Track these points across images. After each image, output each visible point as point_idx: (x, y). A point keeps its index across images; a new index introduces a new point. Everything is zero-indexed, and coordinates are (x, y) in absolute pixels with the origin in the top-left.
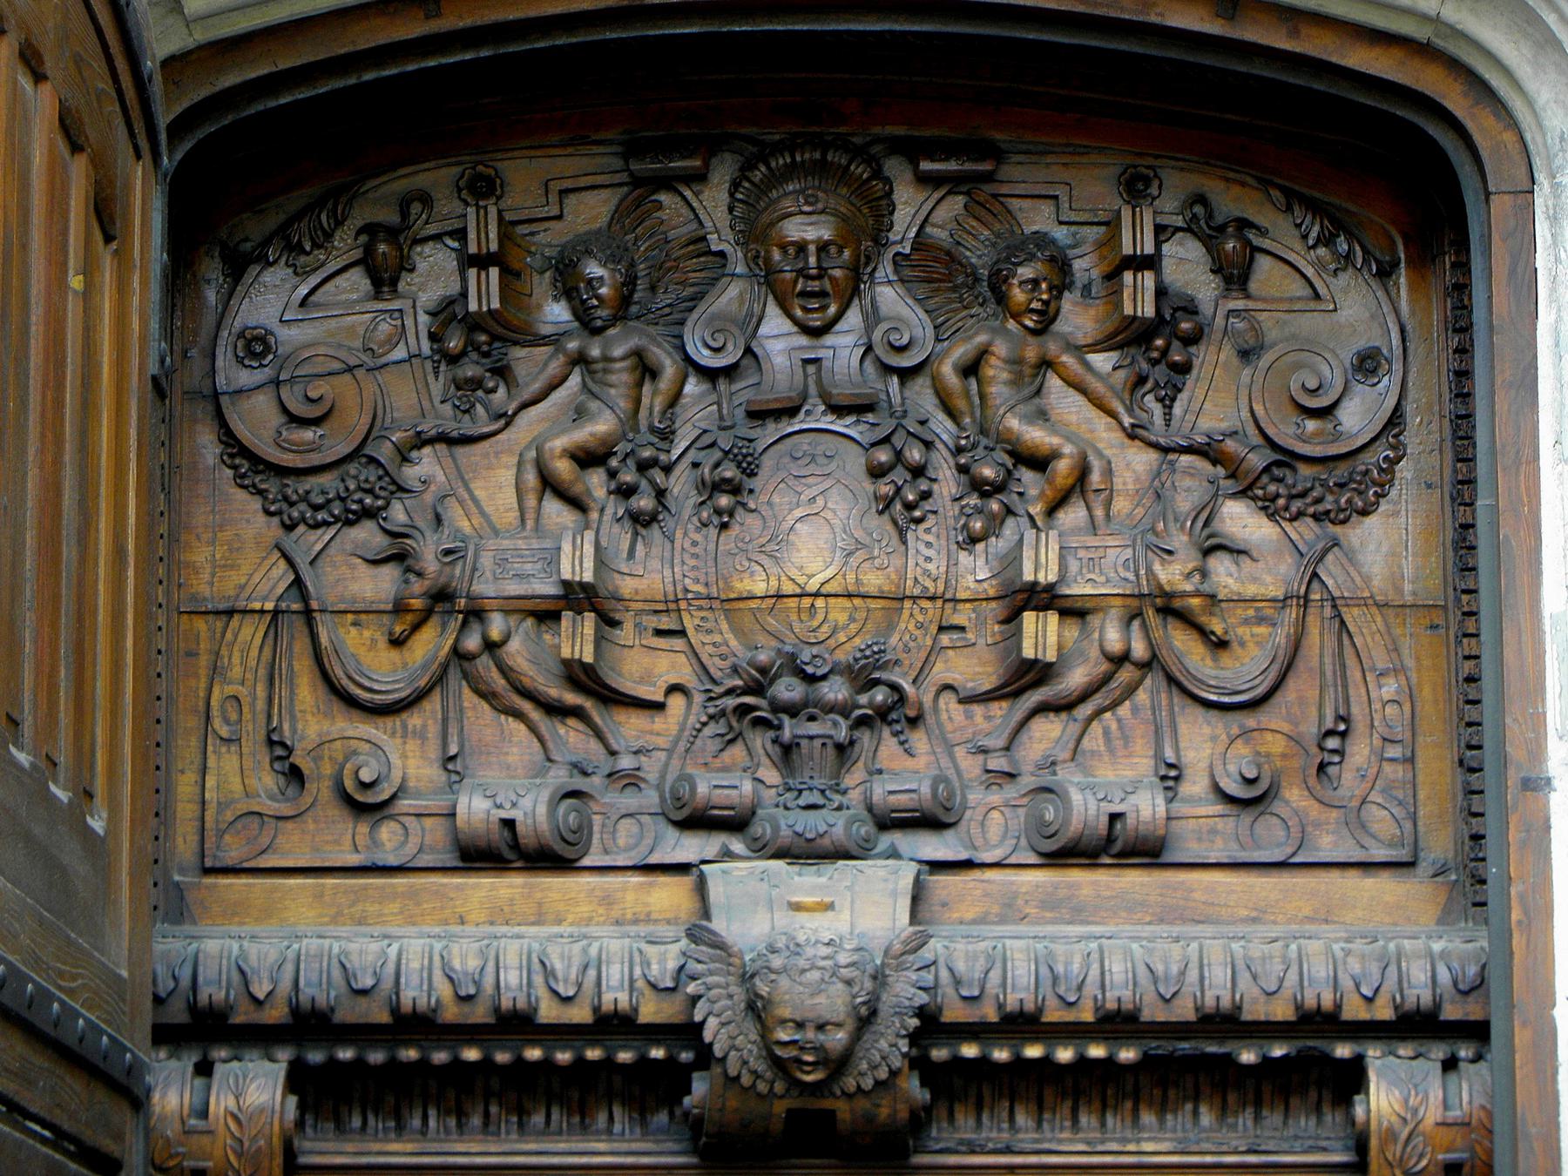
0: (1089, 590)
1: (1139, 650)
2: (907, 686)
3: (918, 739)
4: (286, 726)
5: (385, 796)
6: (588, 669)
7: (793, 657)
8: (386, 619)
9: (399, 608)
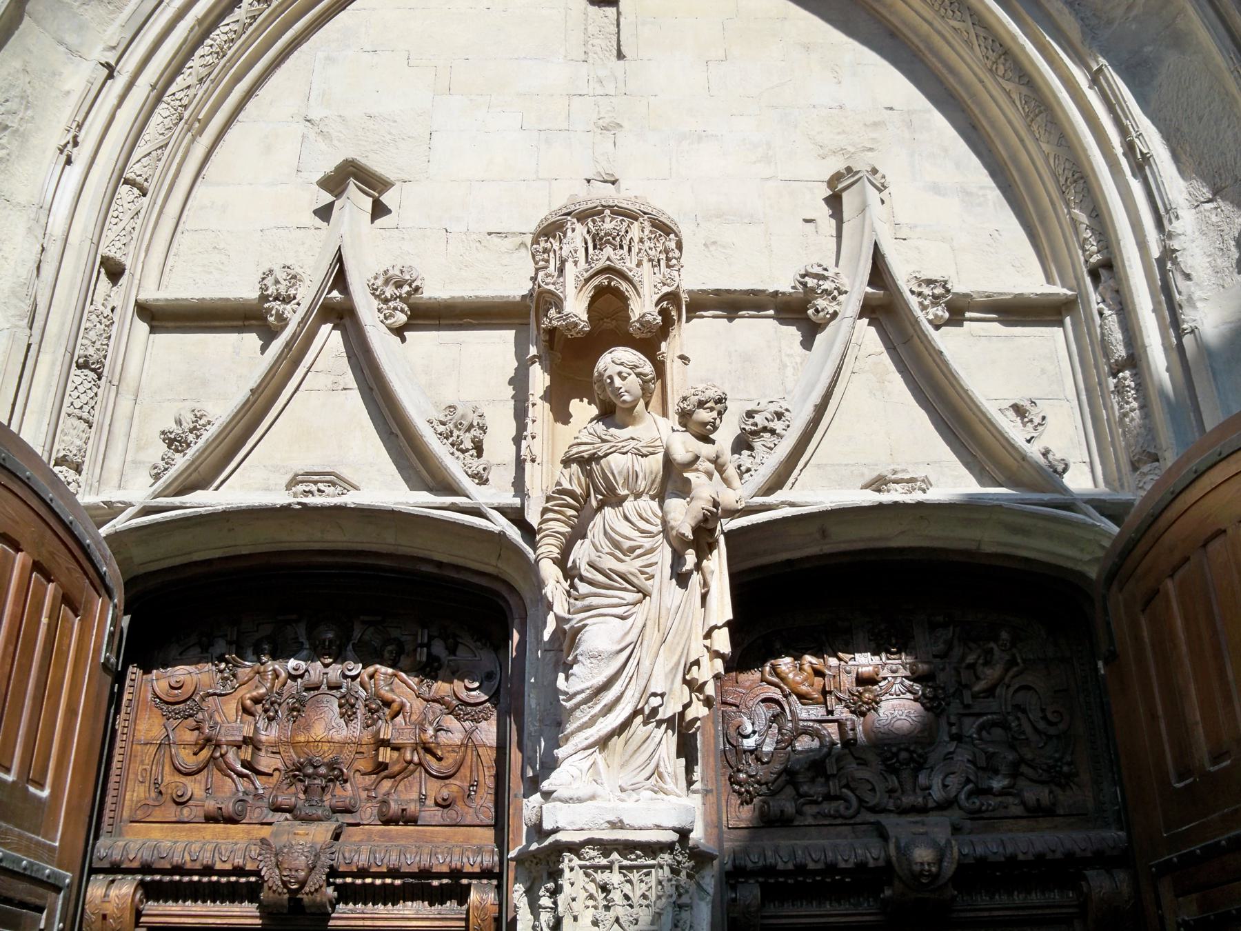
0: (401, 742)
1: (416, 759)
2: (345, 770)
3: (348, 785)
4: (160, 778)
5: (185, 800)
6: (248, 762)
7: (310, 760)
8: (193, 747)
9: (196, 744)
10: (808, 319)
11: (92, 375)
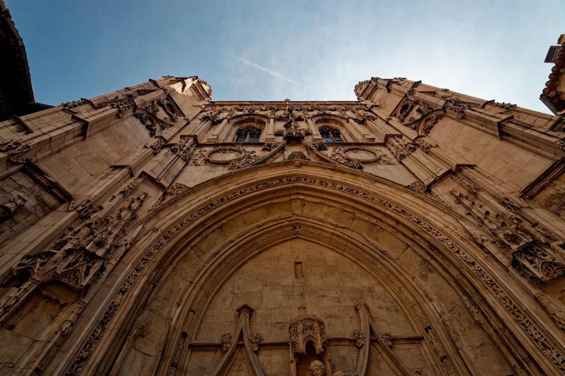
10: (356, 345)
11: (175, 368)
